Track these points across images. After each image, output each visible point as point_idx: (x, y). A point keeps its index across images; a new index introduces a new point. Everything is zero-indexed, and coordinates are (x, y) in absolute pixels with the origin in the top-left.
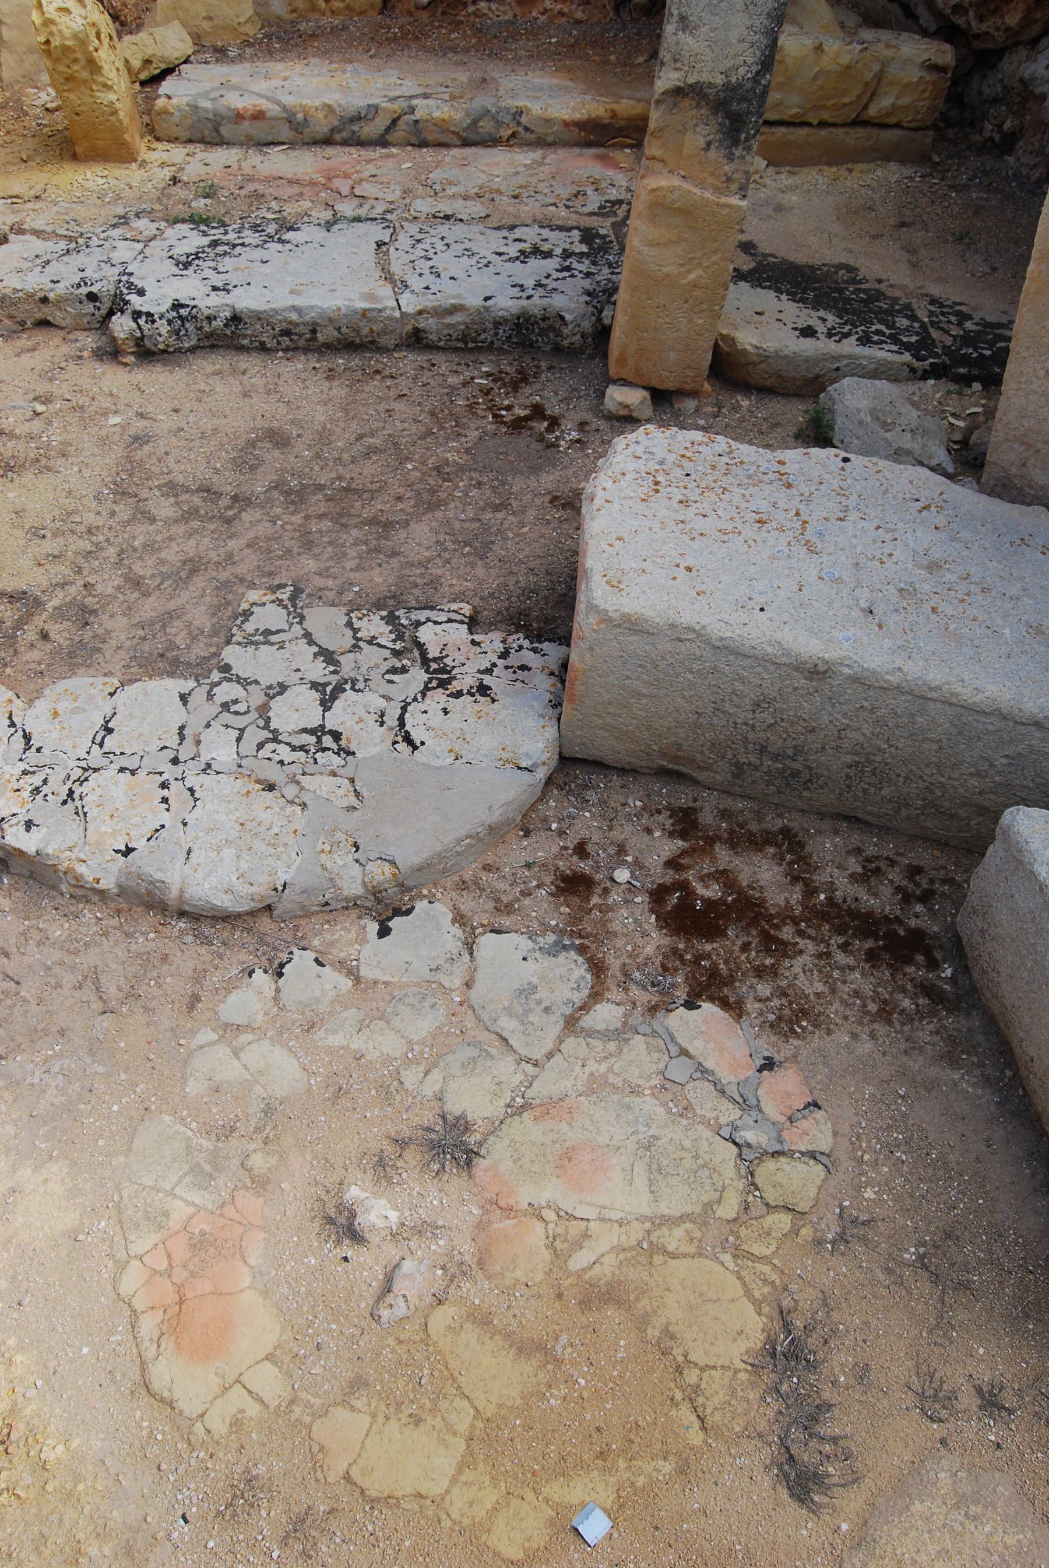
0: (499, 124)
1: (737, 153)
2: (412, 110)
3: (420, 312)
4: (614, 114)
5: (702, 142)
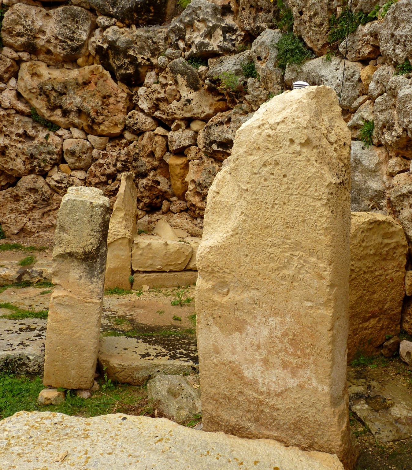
1: (94, 280)
5: (77, 276)
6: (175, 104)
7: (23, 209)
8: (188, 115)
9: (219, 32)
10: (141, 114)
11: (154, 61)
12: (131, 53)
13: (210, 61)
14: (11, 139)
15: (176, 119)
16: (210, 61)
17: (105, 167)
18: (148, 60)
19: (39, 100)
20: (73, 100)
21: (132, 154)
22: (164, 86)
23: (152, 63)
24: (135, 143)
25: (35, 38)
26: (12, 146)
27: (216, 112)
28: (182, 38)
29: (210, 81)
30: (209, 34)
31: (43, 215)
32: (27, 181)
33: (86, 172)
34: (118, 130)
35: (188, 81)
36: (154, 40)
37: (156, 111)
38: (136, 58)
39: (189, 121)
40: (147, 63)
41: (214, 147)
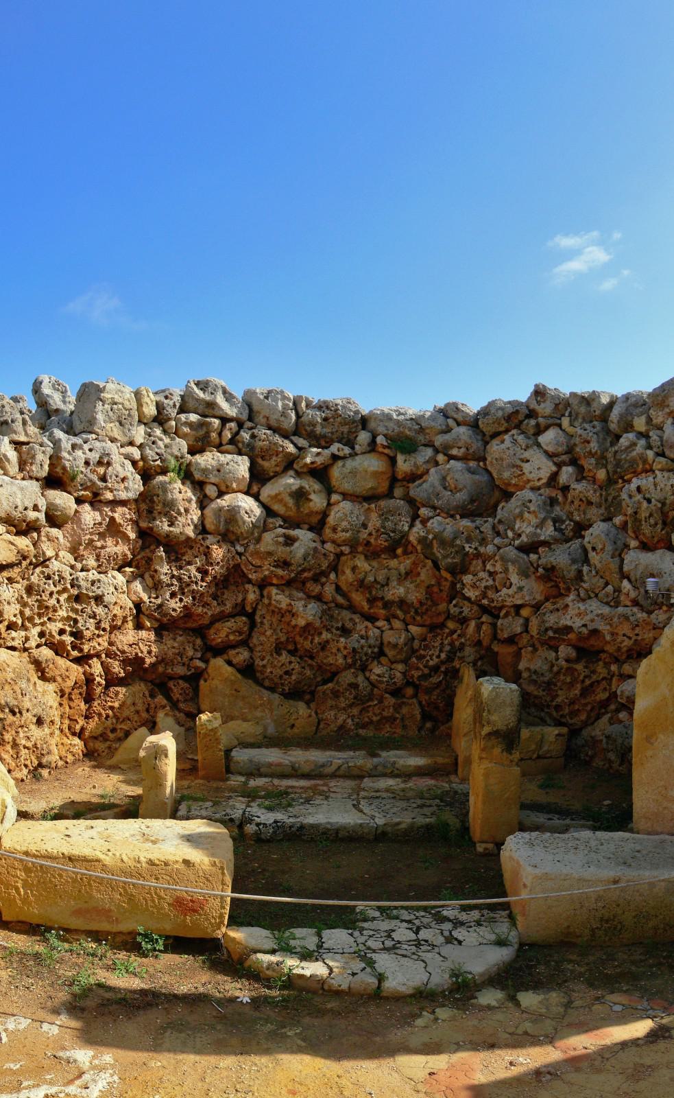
0: (385, 766)
2: (347, 763)
3: (385, 825)
4: (436, 763)
6: (505, 591)
7: (343, 705)
8: (519, 602)
9: (550, 523)
10: (466, 602)
11: (482, 550)
12: (458, 542)
13: (541, 550)
14: (332, 633)
15: (507, 606)
16: (541, 550)
17: (428, 658)
18: (476, 549)
19: (359, 593)
20: (397, 591)
21: (457, 643)
22: (491, 574)
23: (479, 551)
24: (459, 632)
25: (359, 532)
26: (333, 640)
27: (547, 599)
28: (513, 529)
29: (544, 568)
30: (541, 525)
31: (361, 711)
32: (347, 677)
33: (406, 664)
34: (441, 619)
35: (518, 570)
36: (481, 529)
37: (483, 599)
38: (464, 547)
39: (518, 608)
40: (475, 552)
41: (550, 633)
